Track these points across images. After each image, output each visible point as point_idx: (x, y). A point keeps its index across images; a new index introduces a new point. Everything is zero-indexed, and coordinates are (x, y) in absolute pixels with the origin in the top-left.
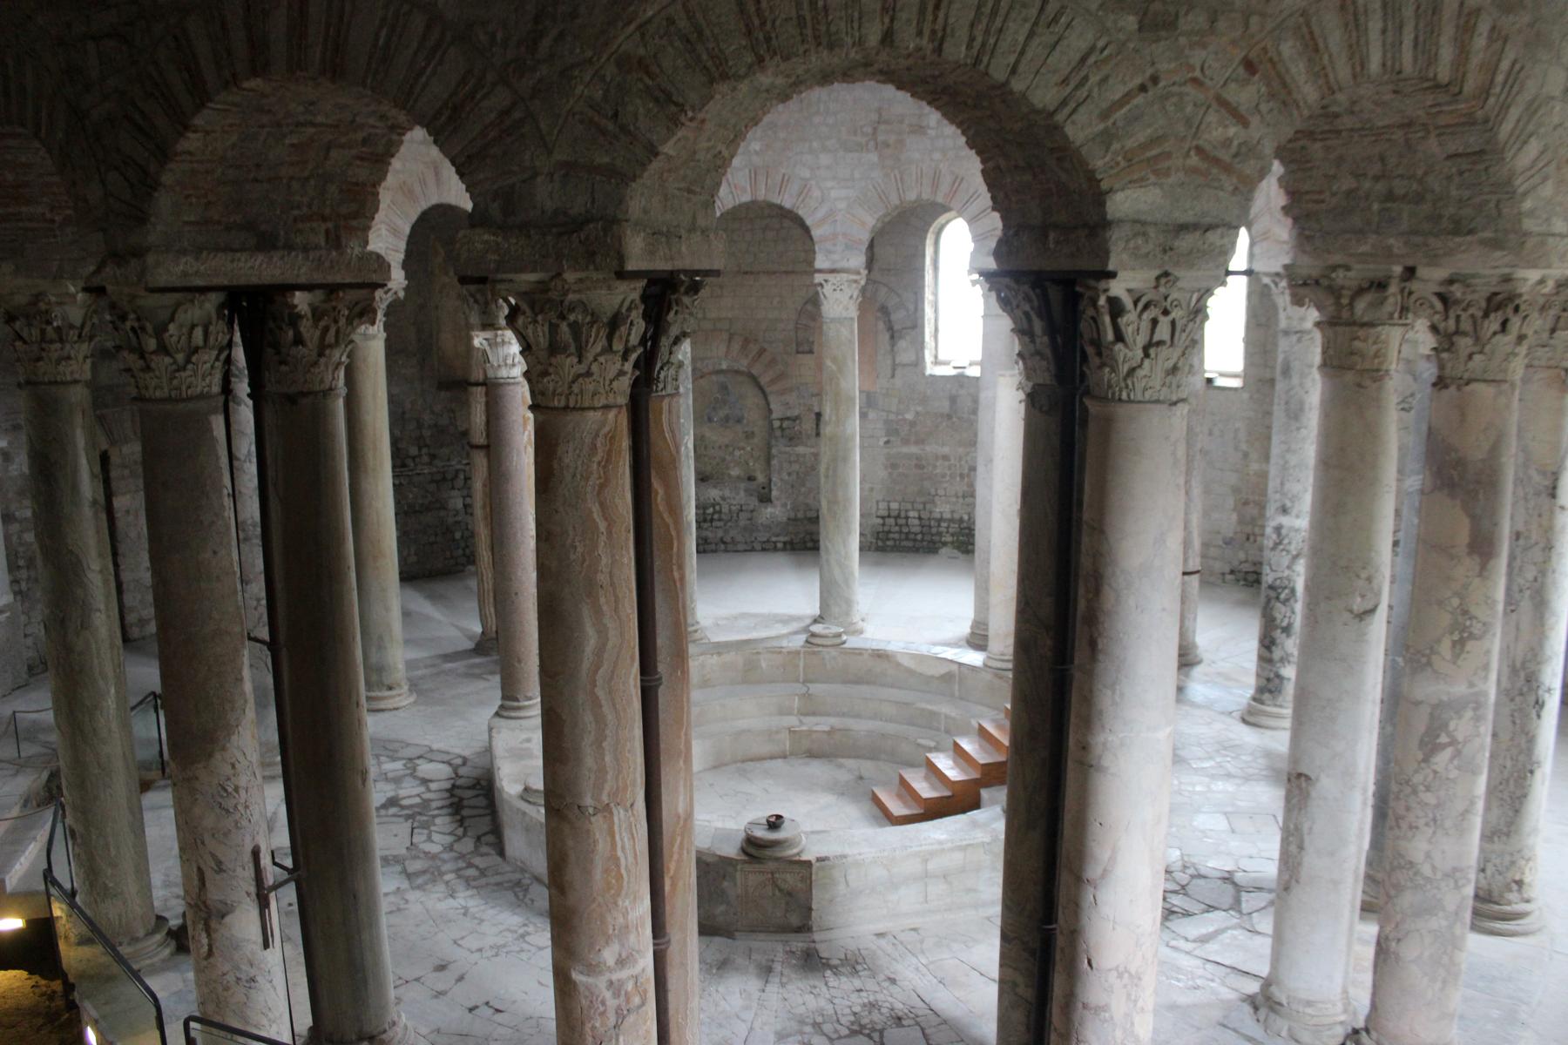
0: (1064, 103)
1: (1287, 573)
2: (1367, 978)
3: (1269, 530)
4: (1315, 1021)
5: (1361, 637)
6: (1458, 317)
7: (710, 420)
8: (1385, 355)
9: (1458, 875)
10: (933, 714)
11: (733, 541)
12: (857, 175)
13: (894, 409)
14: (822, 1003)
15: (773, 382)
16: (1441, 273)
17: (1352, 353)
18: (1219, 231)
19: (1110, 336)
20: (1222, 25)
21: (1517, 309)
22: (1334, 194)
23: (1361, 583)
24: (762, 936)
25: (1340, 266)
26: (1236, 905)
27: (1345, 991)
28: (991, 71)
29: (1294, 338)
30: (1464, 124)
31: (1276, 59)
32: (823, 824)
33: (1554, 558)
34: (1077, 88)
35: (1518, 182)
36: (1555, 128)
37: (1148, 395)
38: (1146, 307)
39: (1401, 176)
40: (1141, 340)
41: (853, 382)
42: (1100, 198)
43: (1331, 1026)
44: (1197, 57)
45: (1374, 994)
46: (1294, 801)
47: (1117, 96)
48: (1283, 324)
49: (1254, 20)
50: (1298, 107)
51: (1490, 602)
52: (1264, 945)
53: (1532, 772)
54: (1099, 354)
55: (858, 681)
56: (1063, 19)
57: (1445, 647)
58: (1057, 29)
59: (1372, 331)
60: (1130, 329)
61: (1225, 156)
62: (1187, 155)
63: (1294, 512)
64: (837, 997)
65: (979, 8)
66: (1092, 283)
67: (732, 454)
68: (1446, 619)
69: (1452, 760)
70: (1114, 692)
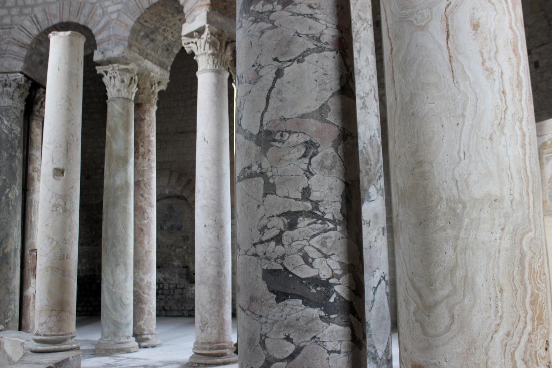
11: (171, 310)
67: (174, 250)
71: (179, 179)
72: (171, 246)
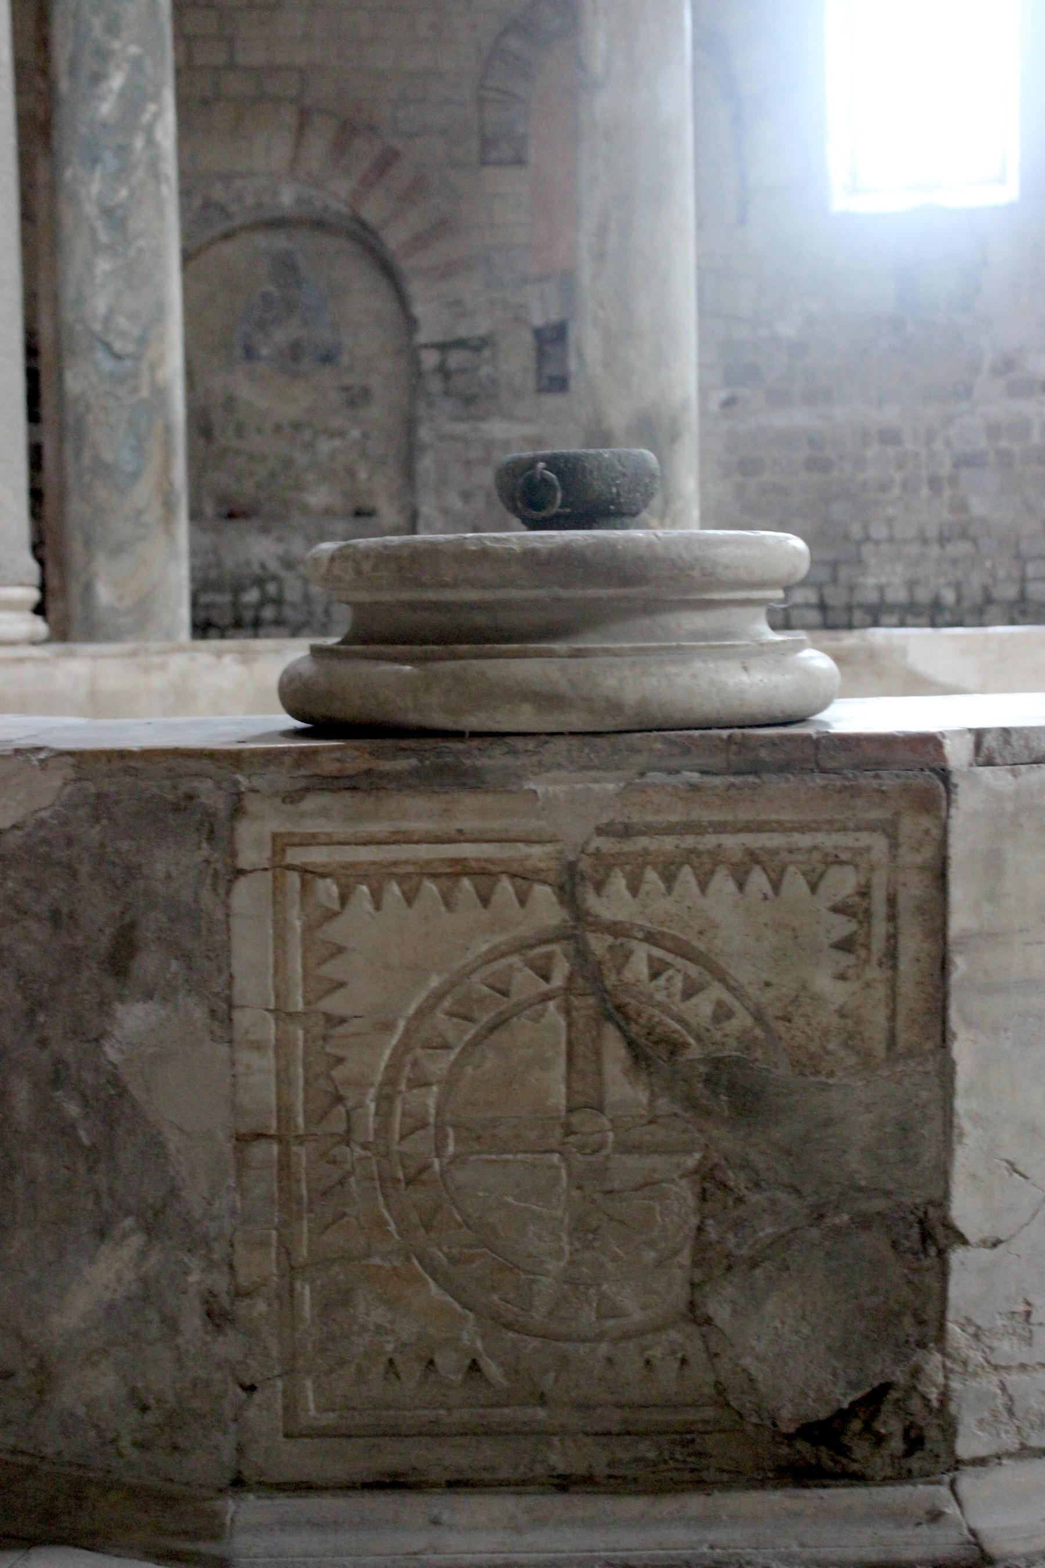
7: (250, 353)
15: (420, 241)
67: (309, 446)
71: (340, 146)
72: (297, 426)
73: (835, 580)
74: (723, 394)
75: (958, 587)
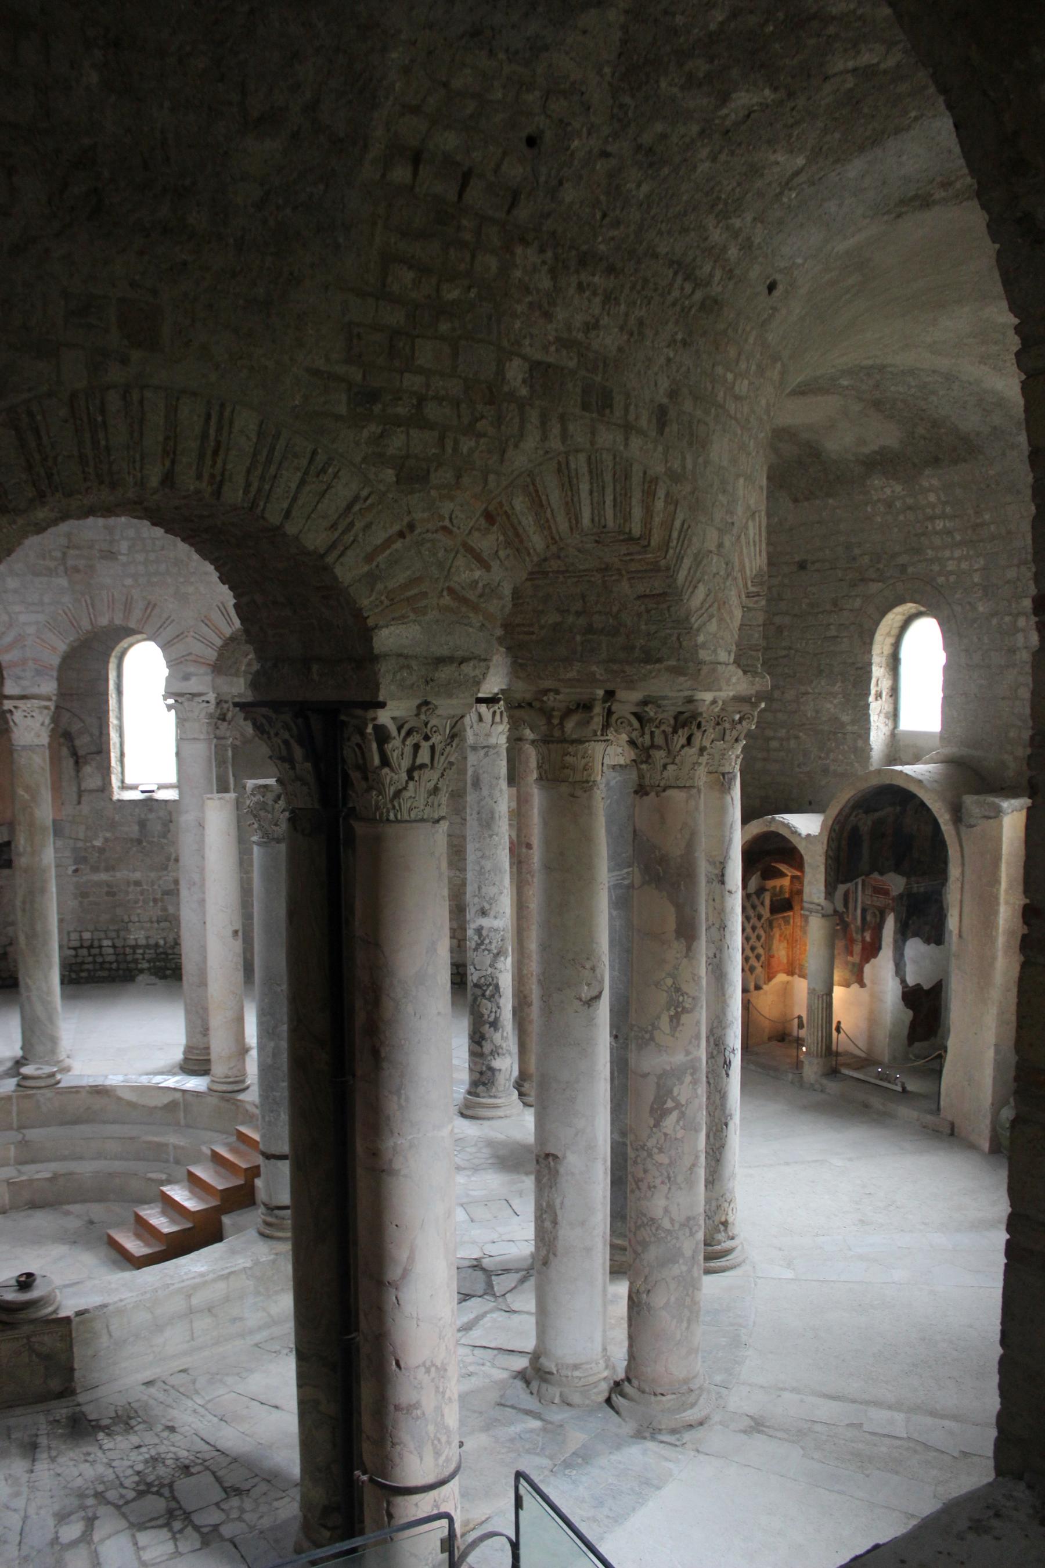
0: (333, 546)
1: (490, 970)
2: (620, 1334)
3: (470, 933)
4: (581, 1384)
5: (591, 1021)
6: (652, 733)
8: (592, 768)
9: (691, 1222)
10: (161, 1147)
12: (46, 600)
13: (81, 835)
14: (100, 1469)
16: (636, 696)
17: (564, 767)
18: (472, 663)
19: (377, 761)
20: (466, 480)
21: (699, 726)
22: (542, 627)
23: (587, 973)
24: (19, 1411)
25: (550, 690)
26: (489, 1290)
27: (605, 1349)
28: (267, 515)
29: (482, 752)
30: (652, 570)
31: (510, 512)
32: (75, 1280)
33: (727, 936)
34: (343, 533)
35: (693, 620)
36: (715, 575)
37: (413, 816)
38: (409, 733)
39: (600, 612)
40: (406, 764)
41: (45, 812)
42: (367, 634)
43: (596, 1384)
44: (447, 507)
45: (631, 1346)
46: (545, 1180)
47: (379, 542)
48: (470, 739)
49: (492, 477)
50: (529, 554)
51: (695, 978)
52: (530, 1323)
53: (726, 1125)
54: (366, 779)
55: (76, 1121)
56: (330, 470)
57: (664, 1023)
58: (325, 478)
59: (581, 747)
60: (395, 754)
61: (471, 595)
62: (441, 596)
63: (492, 914)
64: (117, 1457)
65: (255, 455)
66: (359, 712)
68: (663, 998)
69: (678, 1122)
70: (399, 1098)
73: (118, 937)
74: (74, 868)
75: (164, 939)
